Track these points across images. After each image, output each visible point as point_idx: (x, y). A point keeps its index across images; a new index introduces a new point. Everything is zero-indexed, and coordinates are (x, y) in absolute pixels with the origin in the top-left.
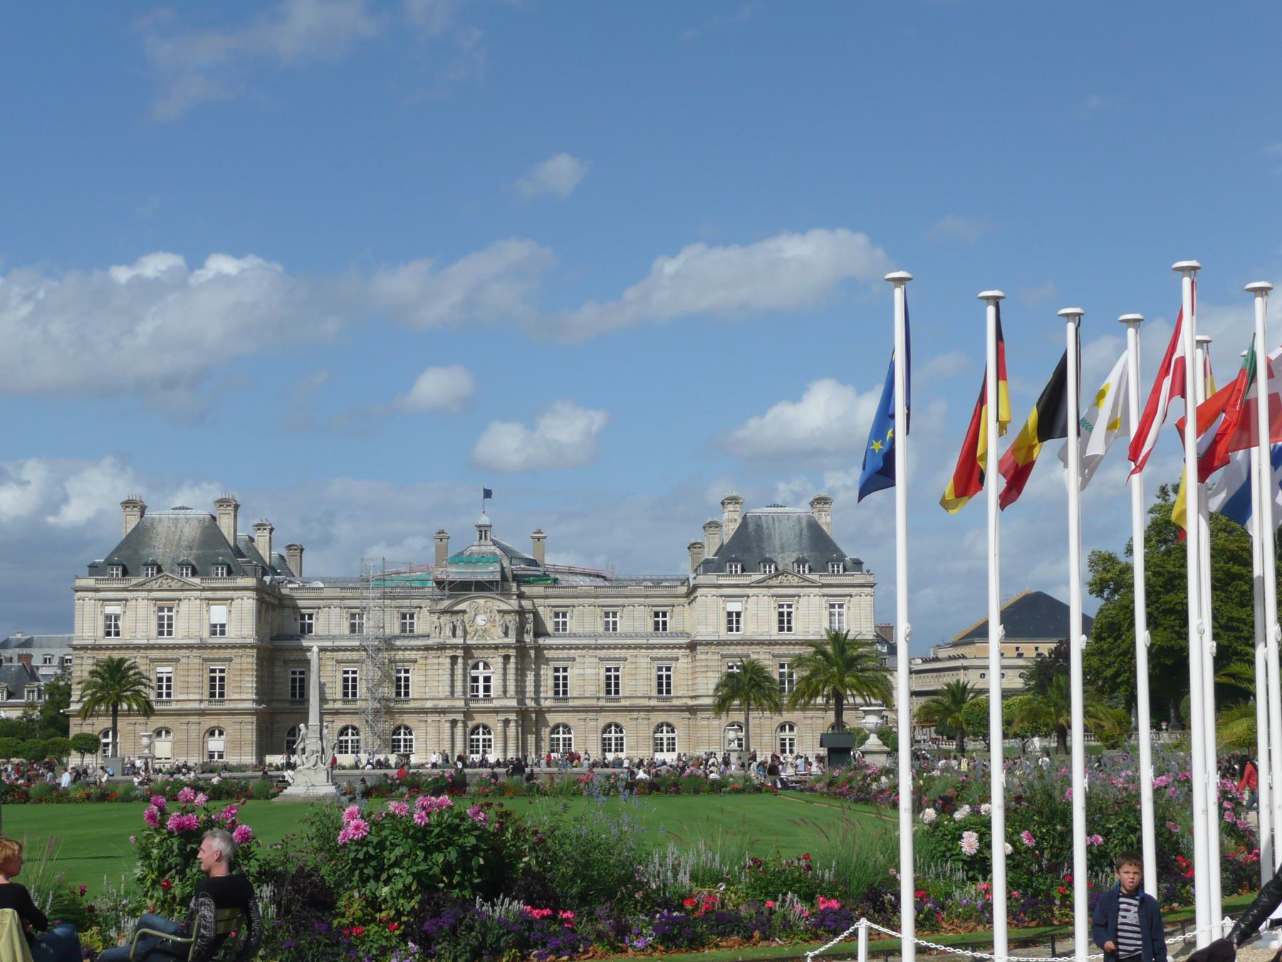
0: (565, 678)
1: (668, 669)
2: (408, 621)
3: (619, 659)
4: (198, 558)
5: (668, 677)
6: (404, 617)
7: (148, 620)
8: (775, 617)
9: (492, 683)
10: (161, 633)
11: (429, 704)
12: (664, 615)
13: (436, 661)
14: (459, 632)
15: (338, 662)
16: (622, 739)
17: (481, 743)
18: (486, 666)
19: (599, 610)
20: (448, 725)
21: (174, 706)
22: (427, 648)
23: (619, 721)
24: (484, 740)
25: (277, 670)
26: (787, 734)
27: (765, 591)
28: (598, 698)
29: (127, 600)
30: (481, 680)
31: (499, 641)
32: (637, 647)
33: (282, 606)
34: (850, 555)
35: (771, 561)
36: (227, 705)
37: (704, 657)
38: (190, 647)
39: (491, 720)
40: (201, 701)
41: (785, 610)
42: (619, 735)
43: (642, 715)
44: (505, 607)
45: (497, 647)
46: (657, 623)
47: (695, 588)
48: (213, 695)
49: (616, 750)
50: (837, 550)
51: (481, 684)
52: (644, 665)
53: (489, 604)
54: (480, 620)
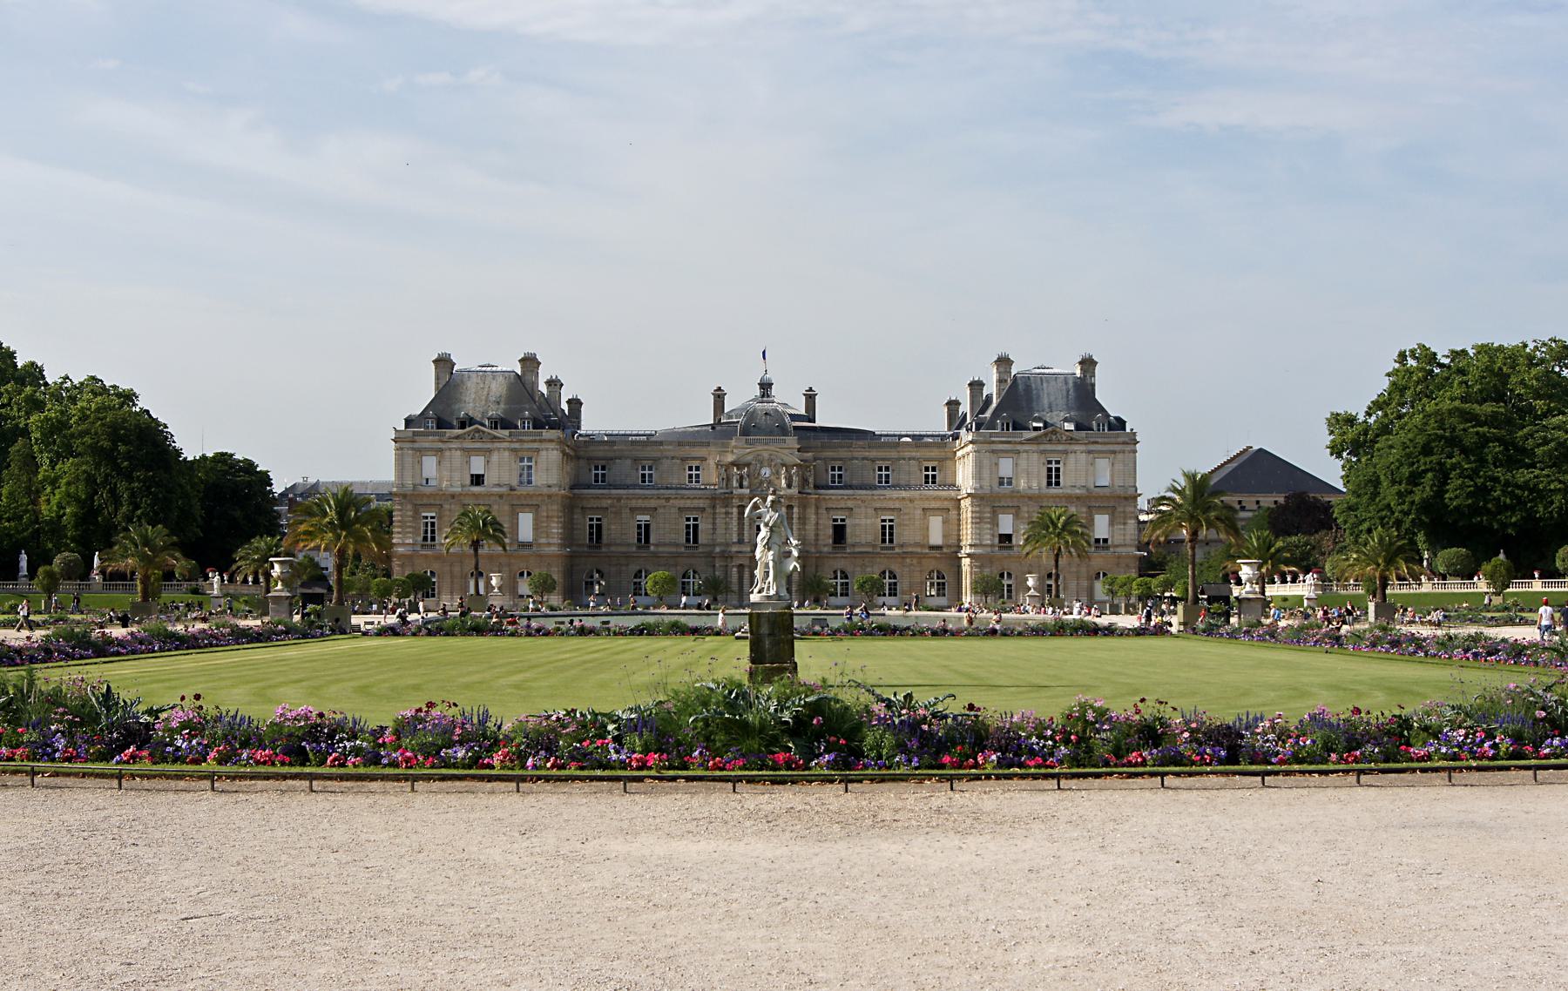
8: (1045, 473)
11: (718, 549)
14: (745, 483)
27: (1034, 447)
29: (441, 450)
33: (578, 458)
34: (1113, 413)
41: (1054, 466)
50: (1103, 410)
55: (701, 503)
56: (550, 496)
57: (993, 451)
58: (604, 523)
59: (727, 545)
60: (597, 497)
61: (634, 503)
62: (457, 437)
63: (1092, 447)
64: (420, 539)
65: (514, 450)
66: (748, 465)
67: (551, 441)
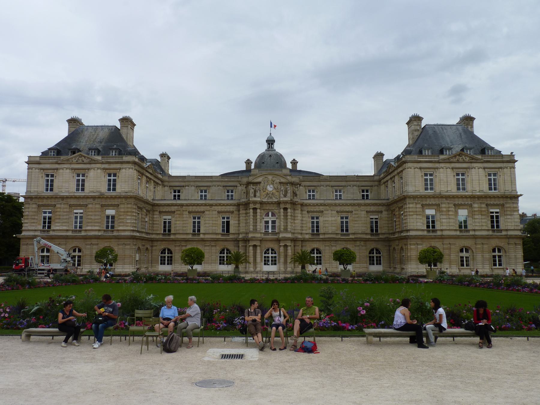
0: (317, 223)
2: (230, 194)
3: (348, 212)
4: (104, 148)
6: (228, 192)
9: (277, 224)
10: (78, 190)
11: (241, 236)
12: (367, 191)
13: (244, 212)
14: (258, 194)
15: (190, 212)
17: (270, 259)
18: (273, 215)
19: (330, 188)
20: (251, 248)
21: (83, 234)
22: (238, 205)
23: (348, 246)
24: (272, 257)
25: (155, 216)
26: (464, 254)
27: (448, 165)
28: (337, 234)
29: (57, 169)
30: (270, 222)
31: (281, 199)
32: (359, 205)
35: (450, 149)
36: (115, 234)
37: (411, 206)
38: (94, 198)
39: (275, 246)
40: (99, 230)
43: (362, 243)
44: (283, 180)
45: (279, 203)
46: (363, 196)
47: (405, 162)
48: (107, 227)
51: (270, 225)
52: (363, 216)
53: (274, 179)
54: (270, 188)
55: (231, 208)
56: (126, 198)
57: (420, 168)
59: (247, 233)
60: (168, 205)
61: (191, 209)
62: (68, 160)
63: (486, 165)
64: (41, 228)
65: (104, 169)
66: (260, 183)
67: (128, 162)
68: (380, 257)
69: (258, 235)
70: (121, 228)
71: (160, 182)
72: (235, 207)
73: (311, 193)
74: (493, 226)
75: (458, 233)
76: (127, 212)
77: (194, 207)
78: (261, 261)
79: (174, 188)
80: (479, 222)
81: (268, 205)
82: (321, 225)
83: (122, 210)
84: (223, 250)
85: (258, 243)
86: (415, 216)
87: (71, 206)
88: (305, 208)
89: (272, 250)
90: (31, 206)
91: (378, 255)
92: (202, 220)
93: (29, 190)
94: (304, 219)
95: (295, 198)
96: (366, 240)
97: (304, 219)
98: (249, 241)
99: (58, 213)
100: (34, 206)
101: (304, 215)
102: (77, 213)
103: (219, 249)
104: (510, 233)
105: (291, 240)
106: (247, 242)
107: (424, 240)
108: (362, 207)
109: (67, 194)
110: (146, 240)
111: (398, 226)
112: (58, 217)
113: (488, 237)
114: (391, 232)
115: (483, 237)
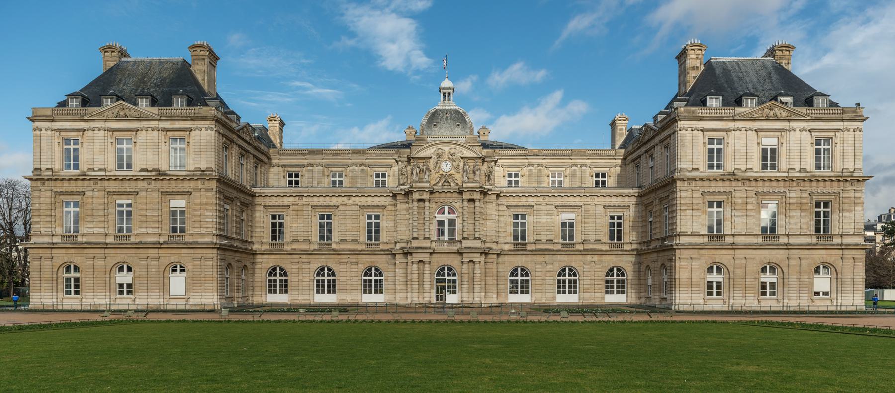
0: (523, 224)
1: (619, 218)
2: (381, 179)
3: (573, 207)
5: (619, 225)
7: (104, 151)
9: (458, 226)
11: (398, 246)
13: (404, 206)
16: (575, 281)
20: (415, 266)
24: (449, 281)
25: (257, 214)
31: (465, 185)
36: (187, 239)
39: (454, 261)
42: (573, 278)
43: (596, 257)
44: (468, 153)
49: (570, 292)
55: (382, 201)
58: (287, 221)
68: (623, 281)
69: (427, 244)
70: (196, 231)
71: (266, 160)
72: (389, 199)
73: (513, 179)
74: (818, 230)
75: (760, 240)
76: (207, 204)
77: (322, 199)
78: (432, 287)
79: (290, 169)
80: (796, 223)
81: (443, 195)
82: (529, 228)
83: (198, 201)
84: (370, 269)
85: (425, 257)
86: (689, 213)
87: (111, 193)
88: (503, 200)
89: (450, 269)
90: (43, 194)
91: (621, 278)
92: (334, 222)
93: (38, 166)
94: (502, 219)
95: (488, 183)
96: (601, 253)
97: (502, 219)
98: (411, 253)
99: (89, 207)
100: (48, 194)
101: (501, 213)
102: (121, 206)
103: (362, 267)
104: (847, 240)
105: (481, 253)
106: (409, 257)
107: (703, 251)
108: (596, 199)
109: (103, 173)
110: (241, 252)
111: (658, 231)
112: (90, 212)
113: (809, 247)
114: (645, 240)
115: (800, 247)
